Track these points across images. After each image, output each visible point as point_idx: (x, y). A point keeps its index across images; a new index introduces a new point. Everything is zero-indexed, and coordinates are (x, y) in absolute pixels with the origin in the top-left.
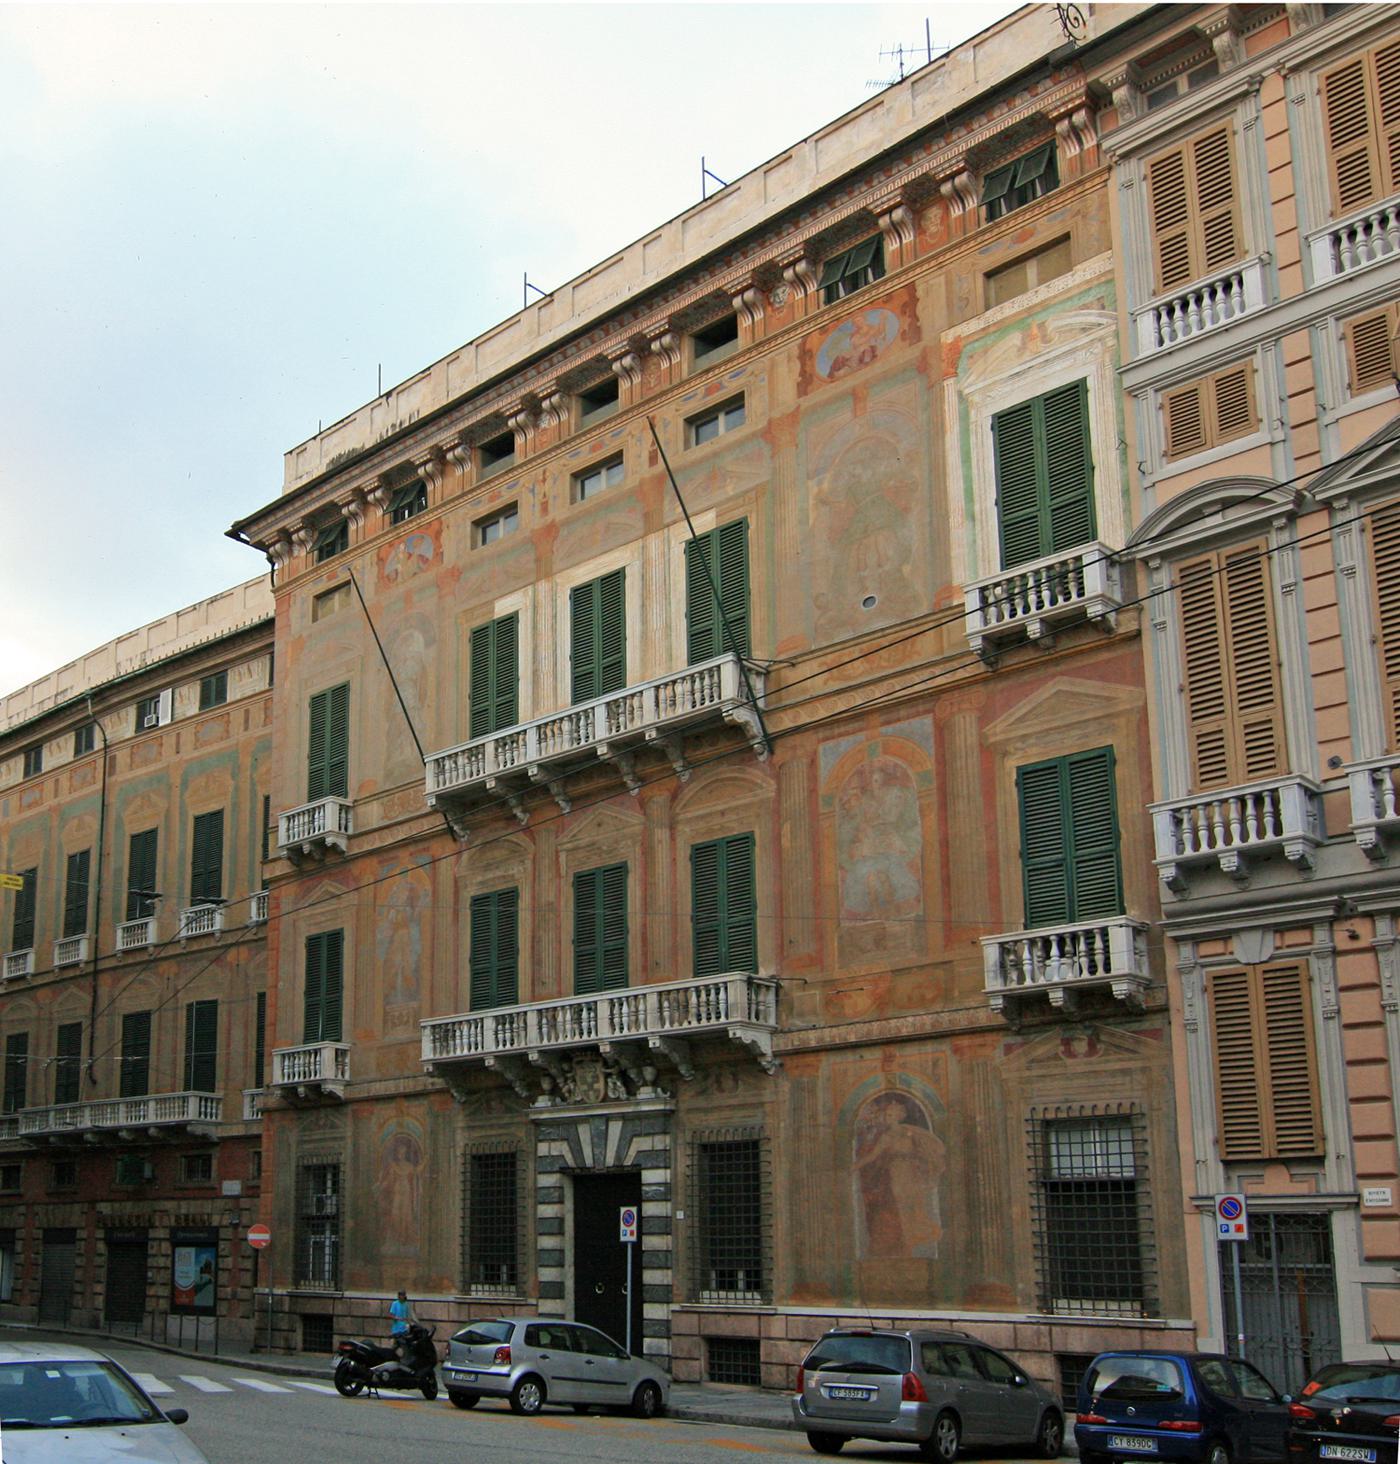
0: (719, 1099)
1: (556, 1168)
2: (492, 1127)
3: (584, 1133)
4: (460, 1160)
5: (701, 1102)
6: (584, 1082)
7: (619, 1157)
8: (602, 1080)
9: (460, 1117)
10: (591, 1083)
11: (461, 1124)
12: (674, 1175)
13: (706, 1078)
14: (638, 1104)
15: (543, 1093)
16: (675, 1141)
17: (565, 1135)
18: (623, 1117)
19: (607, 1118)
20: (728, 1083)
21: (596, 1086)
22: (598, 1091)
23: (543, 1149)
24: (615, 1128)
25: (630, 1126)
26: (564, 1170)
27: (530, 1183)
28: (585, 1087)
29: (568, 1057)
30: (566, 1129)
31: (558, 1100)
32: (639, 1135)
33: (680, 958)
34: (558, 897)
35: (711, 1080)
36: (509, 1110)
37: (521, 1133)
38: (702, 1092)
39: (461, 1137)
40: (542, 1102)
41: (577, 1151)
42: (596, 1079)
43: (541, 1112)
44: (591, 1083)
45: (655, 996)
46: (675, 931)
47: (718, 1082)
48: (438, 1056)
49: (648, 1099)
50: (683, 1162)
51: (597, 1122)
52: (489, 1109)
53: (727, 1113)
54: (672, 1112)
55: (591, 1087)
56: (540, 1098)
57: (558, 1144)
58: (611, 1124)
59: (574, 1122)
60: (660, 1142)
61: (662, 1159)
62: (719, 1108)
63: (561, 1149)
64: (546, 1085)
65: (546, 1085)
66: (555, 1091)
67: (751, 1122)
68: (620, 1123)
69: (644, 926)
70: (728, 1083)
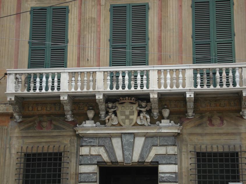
0: (210, 129)
1: (95, 161)
2: (43, 137)
3: (116, 143)
4: (14, 156)
5: (199, 130)
6: (123, 113)
7: (141, 156)
8: (136, 114)
9: (17, 130)
10: (129, 114)
11: (15, 135)
12: (180, 169)
13: (202, 117)
14: (160, 128)
15: (88, 119)
16: (180, 150)
17: (101, 143)
18: (147, 136)
19: (134, 135)
20: (217, 121)
21: (131, 117)
22: (132, 120)
23: (84, 151)
24: (139, 142)
25: (150, 140)
26: (98, 163)
27: (72, 170)
28: (124, 117)
29: (112, 100)
30: (104, 141)
31: (98, 123)
32: (156, 146)
33: (184, 57)
34: (99, 16)
35: (205, 119)
36: (56, 128)
37: (66, 141)
38: (199, 125)
39: (15, 143)
40: (89, 124)
41: (111, 151)
42: (132, 113)
43: (88, 130)
44: (129, 114)
45: (192, 71)
46: (181, 42)
47: (210, 120)
48: (19, 92)
49: (167, 127)
50: (188, 162)
51: (128, 137)
52: (41, 127)
53: (215, 137)
54: (179, 134)
55: (127, 117)
56: (87, 122)
57: (97, 148)
58: (137, 139)
59: (110, 137)
60: (172, 150)
61: (169, 159)
62: (212, 134)
63: (101, 151)
64: (91, 114)
65: (91, 114)
66: (96, 118)
67: (232, 142)
68: (143, 139)
69: (160, 37)
70: (217, 121)
